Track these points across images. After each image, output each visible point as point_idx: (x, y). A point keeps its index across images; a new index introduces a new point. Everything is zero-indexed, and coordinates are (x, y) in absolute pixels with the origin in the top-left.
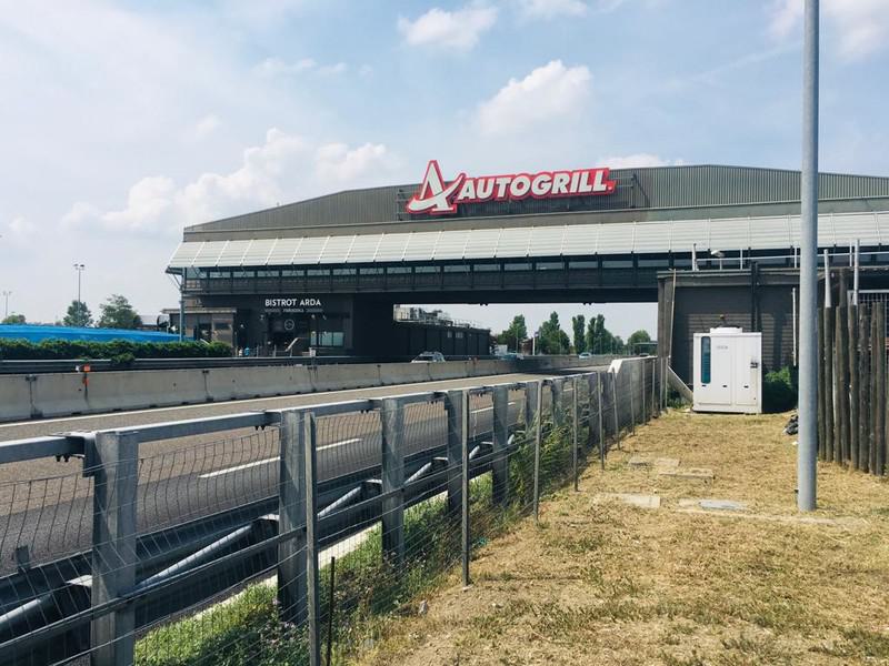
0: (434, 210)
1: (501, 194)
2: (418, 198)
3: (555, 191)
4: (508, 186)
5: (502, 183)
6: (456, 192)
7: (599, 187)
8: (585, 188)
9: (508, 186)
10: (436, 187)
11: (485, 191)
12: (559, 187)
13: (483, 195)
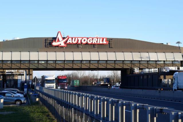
0: (60, 45)
1: (79, 42)
2: (55, 42)
3: (93, 43)
4: (81, 40)
5: (80, 39)
6: (67, 41)
7: (105, 42)
8: (101, 42)
9: (81, 40)
10: (61, 39)
11: (75, 41)
12: (95, 41)
13: (74, 42)
